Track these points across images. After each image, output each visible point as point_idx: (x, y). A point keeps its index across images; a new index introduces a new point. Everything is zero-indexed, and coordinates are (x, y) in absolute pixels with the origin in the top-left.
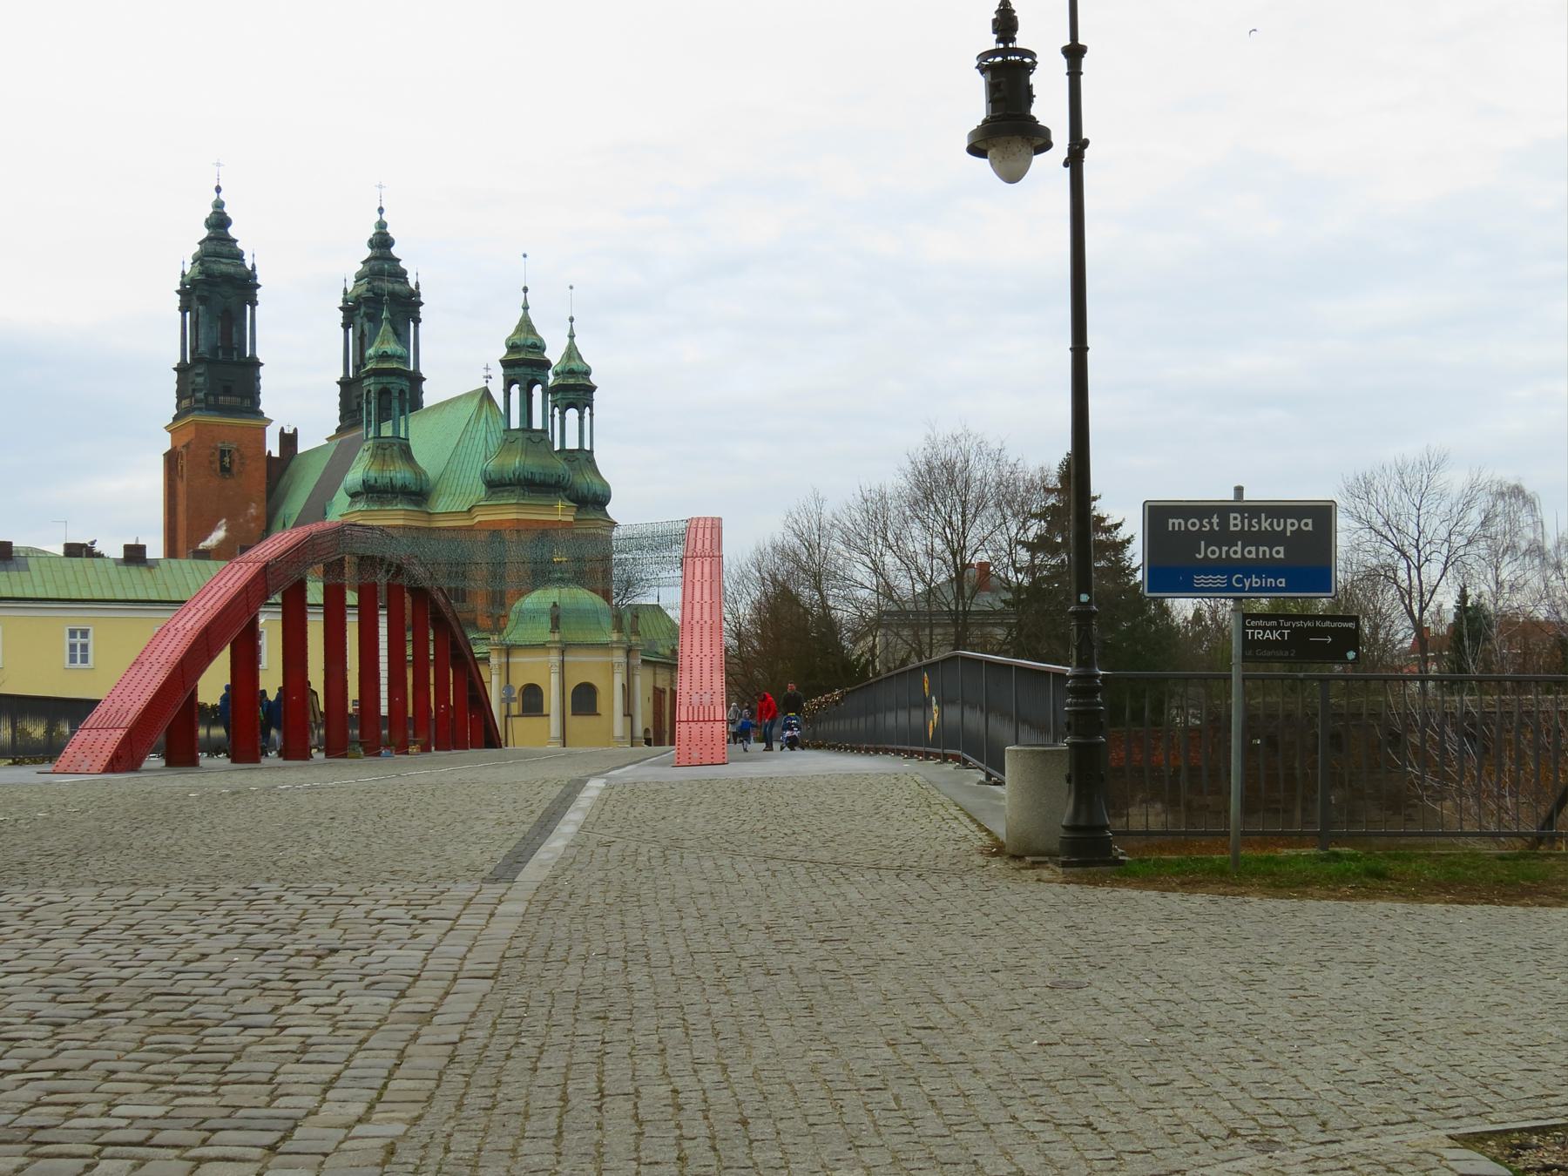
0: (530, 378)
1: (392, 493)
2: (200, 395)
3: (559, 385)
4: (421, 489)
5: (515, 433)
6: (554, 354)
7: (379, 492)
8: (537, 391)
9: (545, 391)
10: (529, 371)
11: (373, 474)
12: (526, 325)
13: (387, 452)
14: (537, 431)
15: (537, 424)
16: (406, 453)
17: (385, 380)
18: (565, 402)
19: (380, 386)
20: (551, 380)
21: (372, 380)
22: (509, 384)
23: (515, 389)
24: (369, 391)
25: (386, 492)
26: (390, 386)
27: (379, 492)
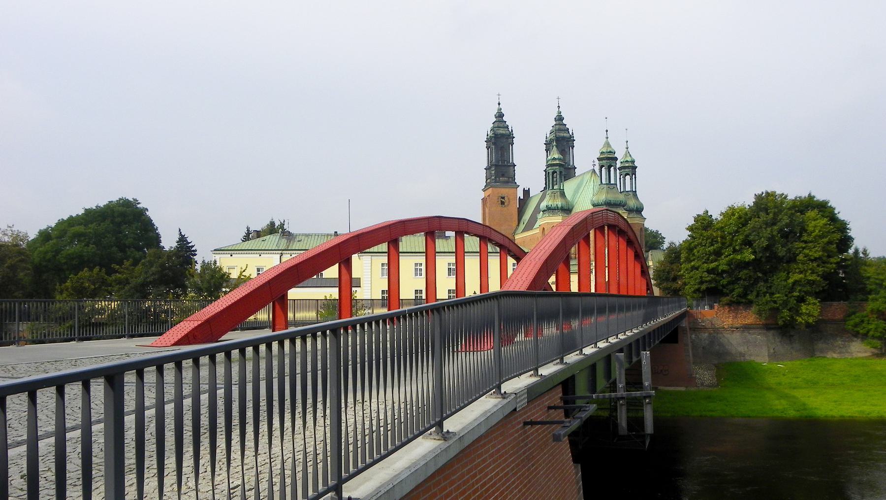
0: (609, 164)
1: (558, 210)
2: (493, 177)
3: (622, 166)
4: (569, 208)
5: (603, 185)
6: (620, 155)
7: (553, 209)
8: (612, 169)
9: (615, 170)
10: (608, 161)
11: (550, 203)
12: (608, 144)
13: (555, 195)
14: (612, 184)
15: (612, 182)
16: (563, 194)
17: (554, 168)
18: (625, 173)
19: (553, 170)
20: (619, 165)
21: (550, 168)
22: (601, 167)
23: (603, 169)
24: (549, 172)
25: (556, 210)
26: (556, 170)
27: (553, 209)
